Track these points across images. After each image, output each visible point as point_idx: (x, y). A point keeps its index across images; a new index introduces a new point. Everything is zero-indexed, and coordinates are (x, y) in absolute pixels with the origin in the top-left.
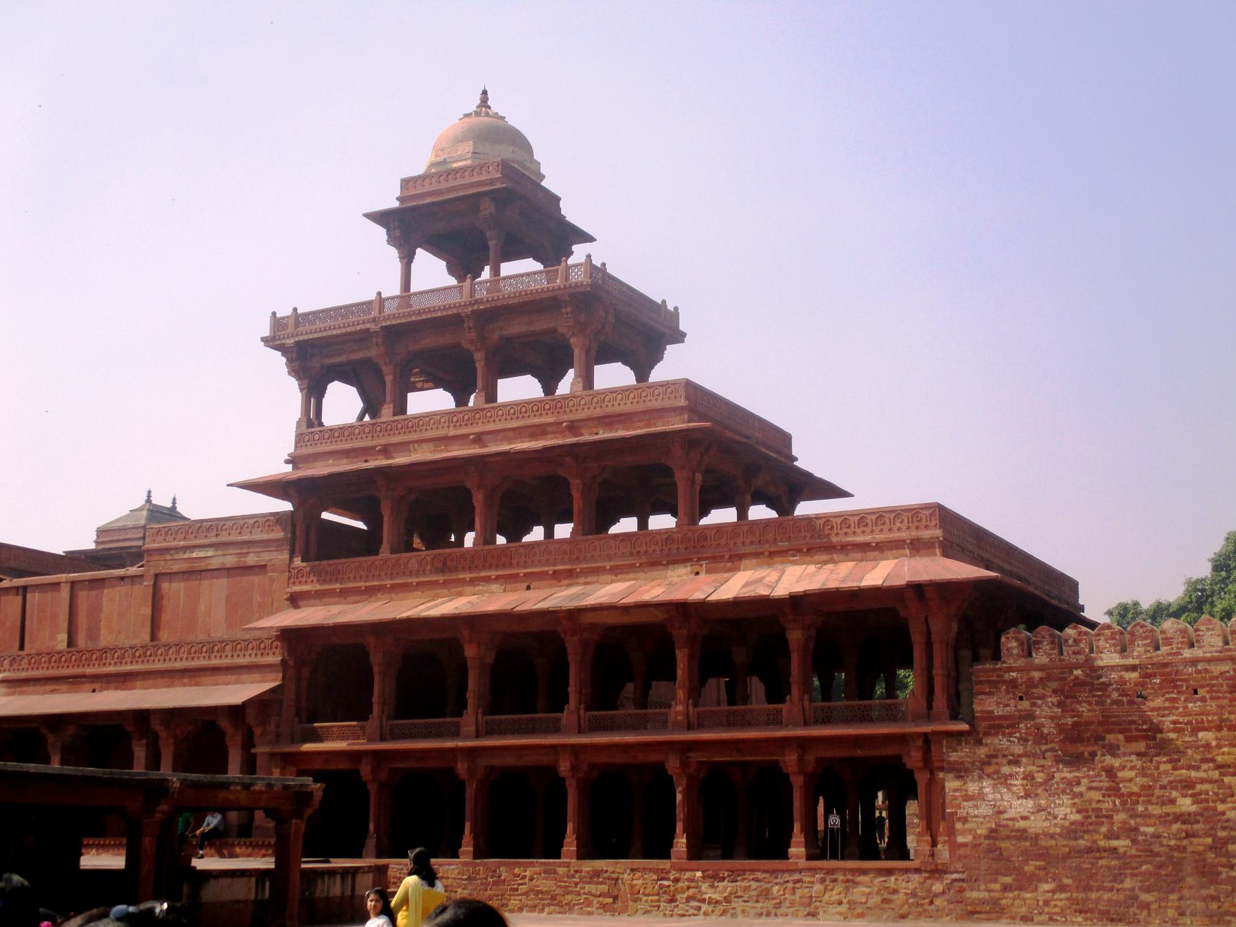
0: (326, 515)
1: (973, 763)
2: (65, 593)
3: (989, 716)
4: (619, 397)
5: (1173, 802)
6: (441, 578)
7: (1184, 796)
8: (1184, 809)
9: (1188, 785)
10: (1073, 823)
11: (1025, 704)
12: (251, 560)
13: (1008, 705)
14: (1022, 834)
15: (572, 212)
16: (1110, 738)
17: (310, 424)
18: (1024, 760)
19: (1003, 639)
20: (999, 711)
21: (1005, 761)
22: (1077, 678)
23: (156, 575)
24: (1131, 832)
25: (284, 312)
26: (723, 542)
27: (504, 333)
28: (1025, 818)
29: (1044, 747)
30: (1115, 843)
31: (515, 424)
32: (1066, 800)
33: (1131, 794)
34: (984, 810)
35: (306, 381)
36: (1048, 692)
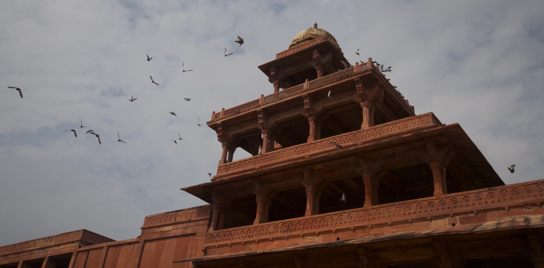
2: (104, 252)
4: (391, 127)
12: (189, 231)
17: (225, 161)
23: (145, 241)
26: (470, 203)
27: (324, 106)
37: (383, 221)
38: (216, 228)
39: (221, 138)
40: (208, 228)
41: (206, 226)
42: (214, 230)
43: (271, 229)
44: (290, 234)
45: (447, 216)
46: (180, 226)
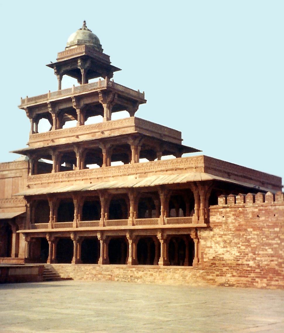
1: (209, 237)
3: (214, 222)
5: (266, 250)
6: (66, 179)
7: (269, 249)
8: (269, 252)
9: (270, 245)
10: (237, 256)
11: (224, 219)
13: (219, 219)
14: (222, 259)
16: (249, 230)
17: (33, 132)
18: (223, 236)
19: (219, 198)
20: (217, 221)
21: (218, 236)
22: (240, 211)
24: (254, 259)
27: (85, 103)
28: (223, 254)
29: (229, 232)
30: (248, 263)
31: (88, 132)
32: (235, 249)
33: (254, 247)
34: (212, 251)
35: (32, 119)
36: (231, 215)
37: (109, 175)
38: (33, 173)
39: (30, 116)
40: (28, 174)
41: (27, 172)
42: (32, 175)
43: (60, 176)
44: (69, 179)
45: (134, 174)
46: (14, 171)
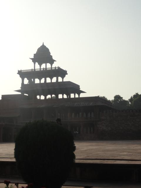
0: (25, 94)
15: (54, 58)
25: (20, 70)
39: (21, 77)
